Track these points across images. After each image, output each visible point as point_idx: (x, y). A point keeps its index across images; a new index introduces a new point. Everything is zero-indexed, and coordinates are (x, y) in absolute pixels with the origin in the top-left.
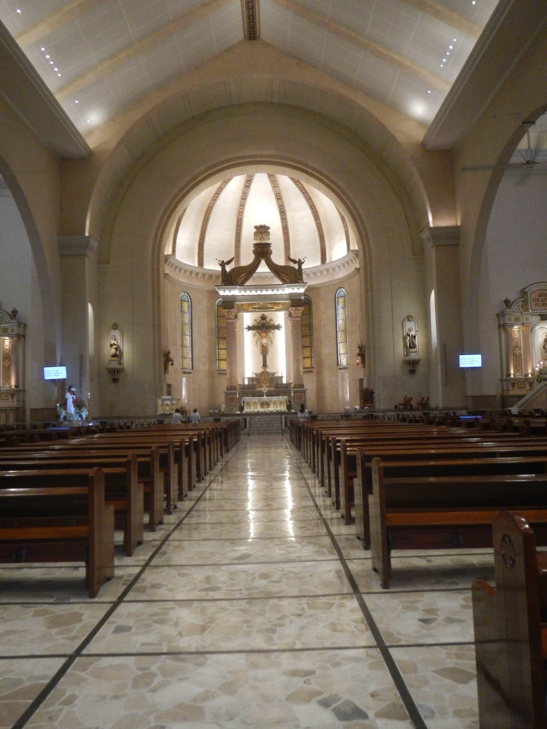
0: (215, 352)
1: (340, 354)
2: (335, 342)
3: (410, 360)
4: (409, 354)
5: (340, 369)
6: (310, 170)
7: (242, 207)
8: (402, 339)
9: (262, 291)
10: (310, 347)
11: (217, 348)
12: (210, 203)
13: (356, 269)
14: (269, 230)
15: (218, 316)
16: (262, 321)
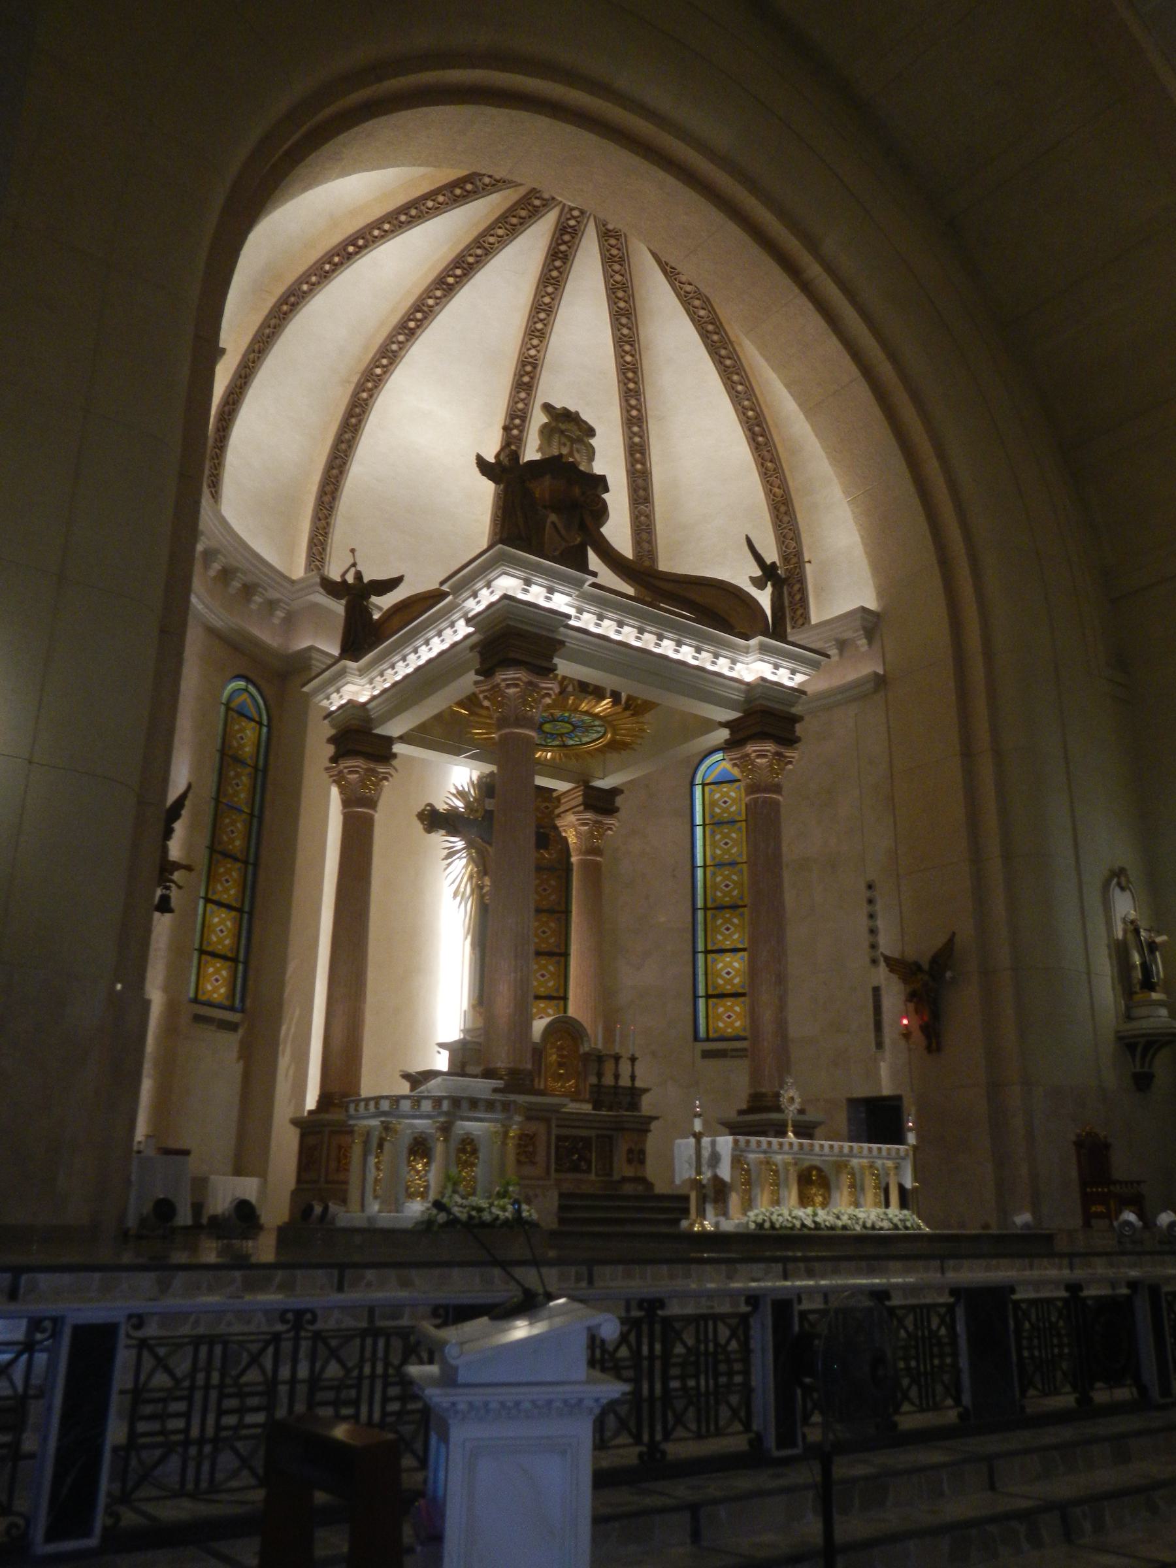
0: (196, 909)
1: (708, 997)
2: (689, 948)
3: (1135, 1036)
4: (1138, 1012)
5: (707, 1054)
6: (814, 271)
7: (385, 361)
8: (1104, 951)
9: (660, 637)
10: (560, 955)
11: (202, 894)
12: (304, 278)
13: (876, 674)
14: (593, 441)
15: (223, 752)
16: (487, 801)
